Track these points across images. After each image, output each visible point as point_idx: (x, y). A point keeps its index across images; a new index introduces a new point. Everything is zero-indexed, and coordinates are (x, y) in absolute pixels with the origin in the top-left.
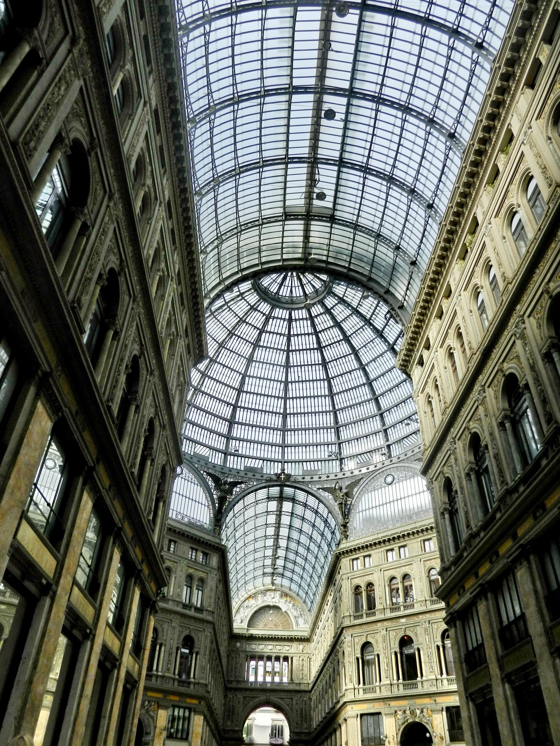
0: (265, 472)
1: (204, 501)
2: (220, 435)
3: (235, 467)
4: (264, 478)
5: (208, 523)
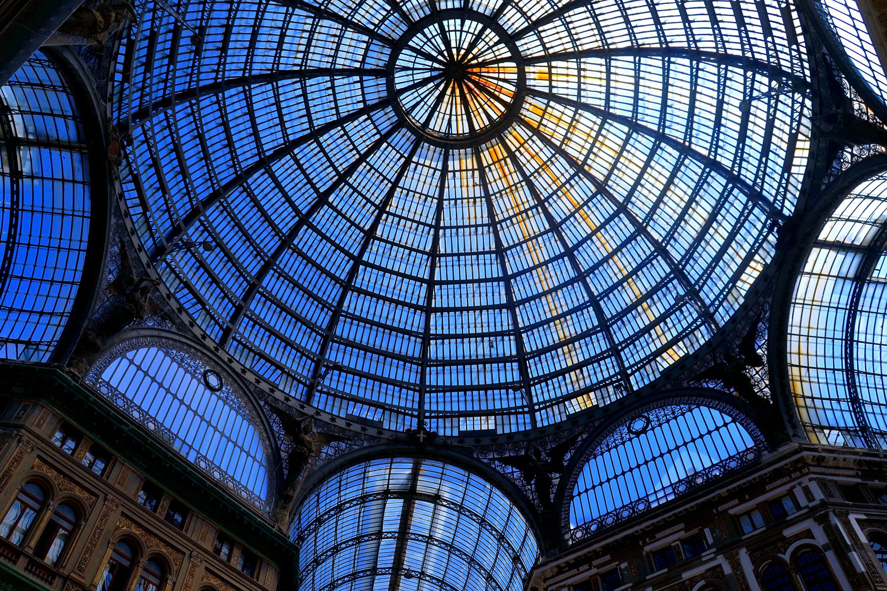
4: (386, 435)
5: (263, 497)
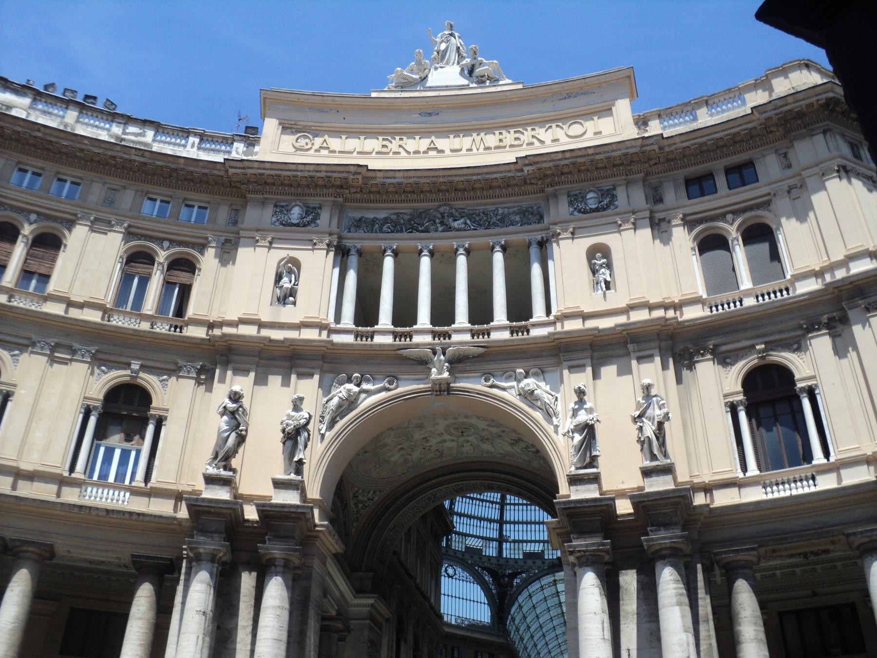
0: (546, 557)
1: (484, 599)
2: (490, 521)
3: (512, 557)
